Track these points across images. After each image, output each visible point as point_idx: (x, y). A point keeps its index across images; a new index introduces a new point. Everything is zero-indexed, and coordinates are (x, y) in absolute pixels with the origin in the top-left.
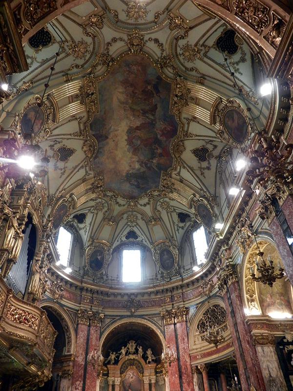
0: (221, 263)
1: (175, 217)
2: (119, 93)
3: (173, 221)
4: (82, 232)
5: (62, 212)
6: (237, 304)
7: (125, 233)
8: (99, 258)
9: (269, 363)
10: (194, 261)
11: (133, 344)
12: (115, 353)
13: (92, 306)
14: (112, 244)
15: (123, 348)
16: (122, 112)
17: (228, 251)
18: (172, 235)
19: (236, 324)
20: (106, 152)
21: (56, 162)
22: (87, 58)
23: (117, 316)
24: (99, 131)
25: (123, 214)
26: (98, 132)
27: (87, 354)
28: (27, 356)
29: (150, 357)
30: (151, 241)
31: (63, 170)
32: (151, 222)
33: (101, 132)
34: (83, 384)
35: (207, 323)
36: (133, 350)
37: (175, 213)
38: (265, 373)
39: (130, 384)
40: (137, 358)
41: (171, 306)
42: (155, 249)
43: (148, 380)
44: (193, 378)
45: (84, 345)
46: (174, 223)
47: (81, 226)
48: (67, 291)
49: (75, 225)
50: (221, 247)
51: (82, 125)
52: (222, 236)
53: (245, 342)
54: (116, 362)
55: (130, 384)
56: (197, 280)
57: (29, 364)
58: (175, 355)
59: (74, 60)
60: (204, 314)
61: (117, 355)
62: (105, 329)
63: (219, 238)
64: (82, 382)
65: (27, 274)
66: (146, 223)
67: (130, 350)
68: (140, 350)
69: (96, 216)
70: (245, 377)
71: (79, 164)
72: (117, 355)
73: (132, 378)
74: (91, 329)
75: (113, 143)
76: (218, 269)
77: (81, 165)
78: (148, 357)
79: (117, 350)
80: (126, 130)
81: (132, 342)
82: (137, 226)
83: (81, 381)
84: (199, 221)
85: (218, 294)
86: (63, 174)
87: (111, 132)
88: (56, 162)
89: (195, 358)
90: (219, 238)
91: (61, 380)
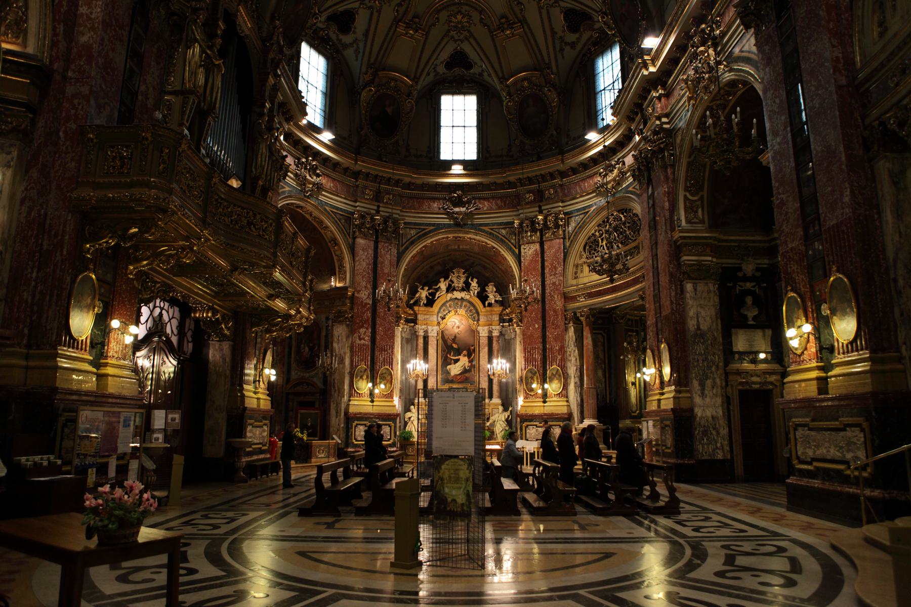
0: (645, 125)
1: (559, 20)
3: (552, 29)
4: (349, 53)
5: (301, 6)
6: (663, 208)
7: (445, 55)
8: (389, 110)
9: (699, 309)
10: (591, 119)
11: (461, 275)
13: (379, 207)
14: (415, 79)
15: (442, 280)
17: (663, 100)
18: (547, 61)
19: (654, 244)
23: (430, 225)
25: (438, 11)
27: (375, 287)
28: (265, 283)
30: (501, 75)
32: (503, 31)
34: (371, 332)
35: (602, 242)
37: (558, 10)
38: (691, 324)
39: (455, 337)
40: (468, 297)
41: (537, 209)
42: (509, 94)
44: (566, 329)
45: (368, 273)
46: (554, 33)
47: (347, 39)
48: (328, 176)
49: (333, 37)
50: (649, 92)
52: (655, 66)
53: (665, 275)
54: (430, 302)
55: (455, 337)
56: (594, 160)
57: (271, 297)
58: (538, 293)
60: (599, 225)
61: (430, 291)
62: (407, 248)
63: (647, 69)
64: (370, 330)
65: (244, 143)
66: (491, 32)
68: (474, 284)
69: (379, 16)
70: (655, 329)
72: (430, 291)
73: (458, 327)
74: (380, 246)
76: (637, 138)
78: (488, 297)
79: (432, 283)
81: (458, 272)
82: (472, 40)
83: (367, 329)
84: (611, 30)
85: (630, 189)
89: (574, 299)
90: (647, 69)
91: (333, 326)
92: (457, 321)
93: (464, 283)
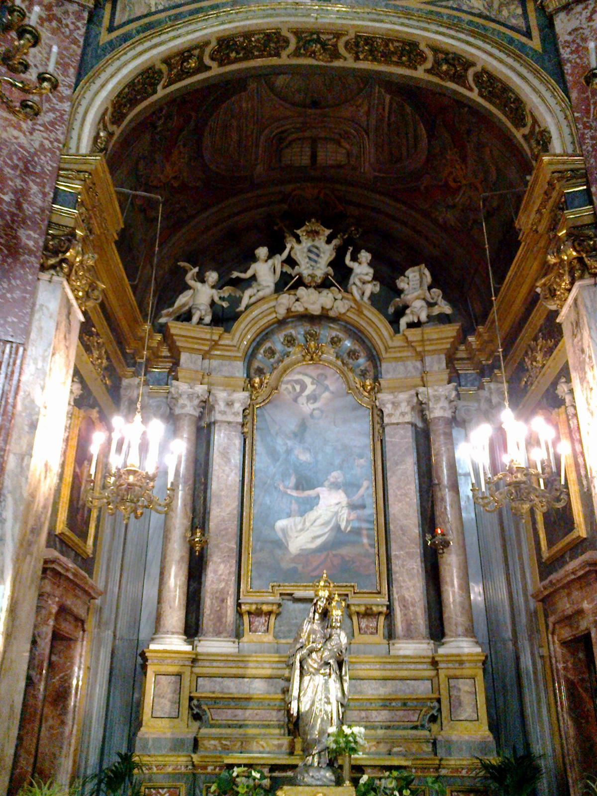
11: (321, 242)
12: (212, 276)
15: (262, 252)
29: (418, 304)
36: (322, 269)
43: (404, 407)
67: (304, 269)
73: (313, 398)
92: (308, 381)
93: (331, 264)
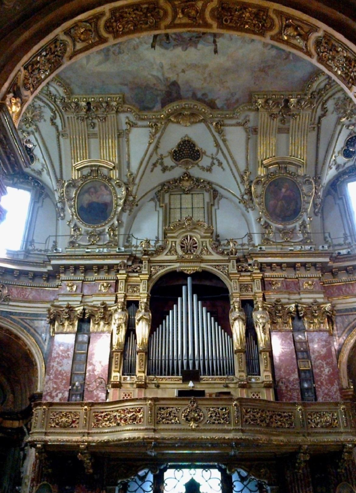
2: (90, 63)
5: (283, 190)
16: (125, 57)
20: (205, 85)
21: (198, 166)
22: (42, 104)
24: (157, 96)
26: (159, 98)
31: (215, 161)
33: (159, 92)
51: (140, 123)
59: (45, 120)
71: (214, 136)
75: (186, 72)
77: (216, 134)
80: (163, 51)
86: (220, 164)
87: (163, 75)
88: (198, 166)
